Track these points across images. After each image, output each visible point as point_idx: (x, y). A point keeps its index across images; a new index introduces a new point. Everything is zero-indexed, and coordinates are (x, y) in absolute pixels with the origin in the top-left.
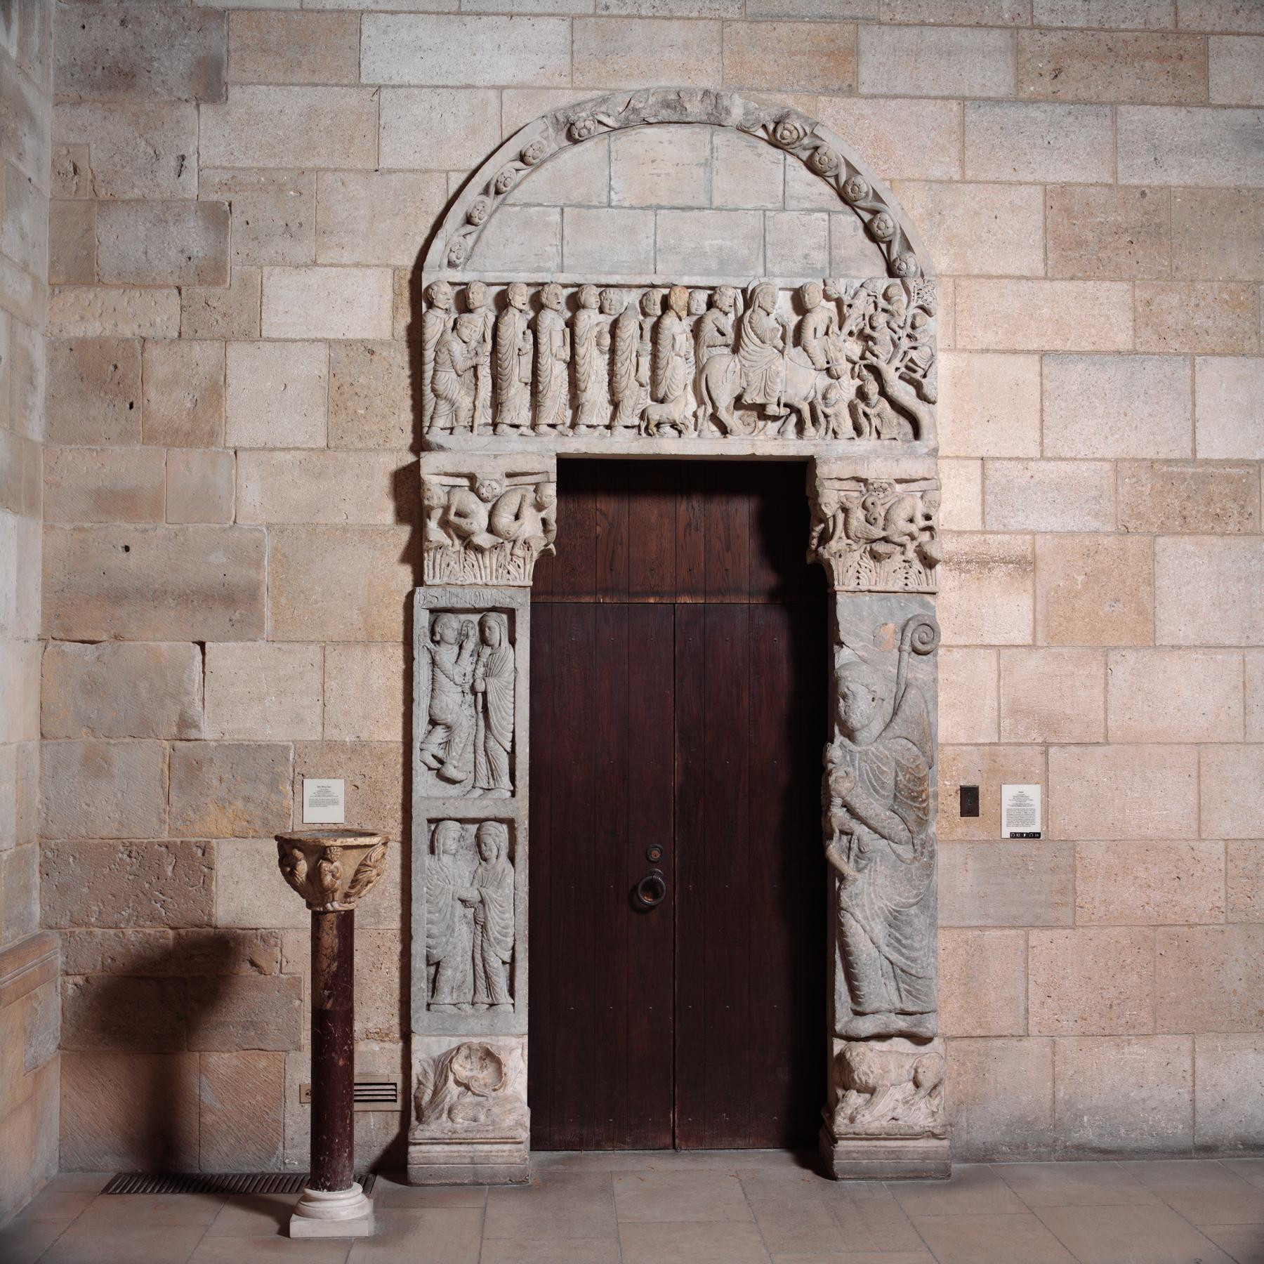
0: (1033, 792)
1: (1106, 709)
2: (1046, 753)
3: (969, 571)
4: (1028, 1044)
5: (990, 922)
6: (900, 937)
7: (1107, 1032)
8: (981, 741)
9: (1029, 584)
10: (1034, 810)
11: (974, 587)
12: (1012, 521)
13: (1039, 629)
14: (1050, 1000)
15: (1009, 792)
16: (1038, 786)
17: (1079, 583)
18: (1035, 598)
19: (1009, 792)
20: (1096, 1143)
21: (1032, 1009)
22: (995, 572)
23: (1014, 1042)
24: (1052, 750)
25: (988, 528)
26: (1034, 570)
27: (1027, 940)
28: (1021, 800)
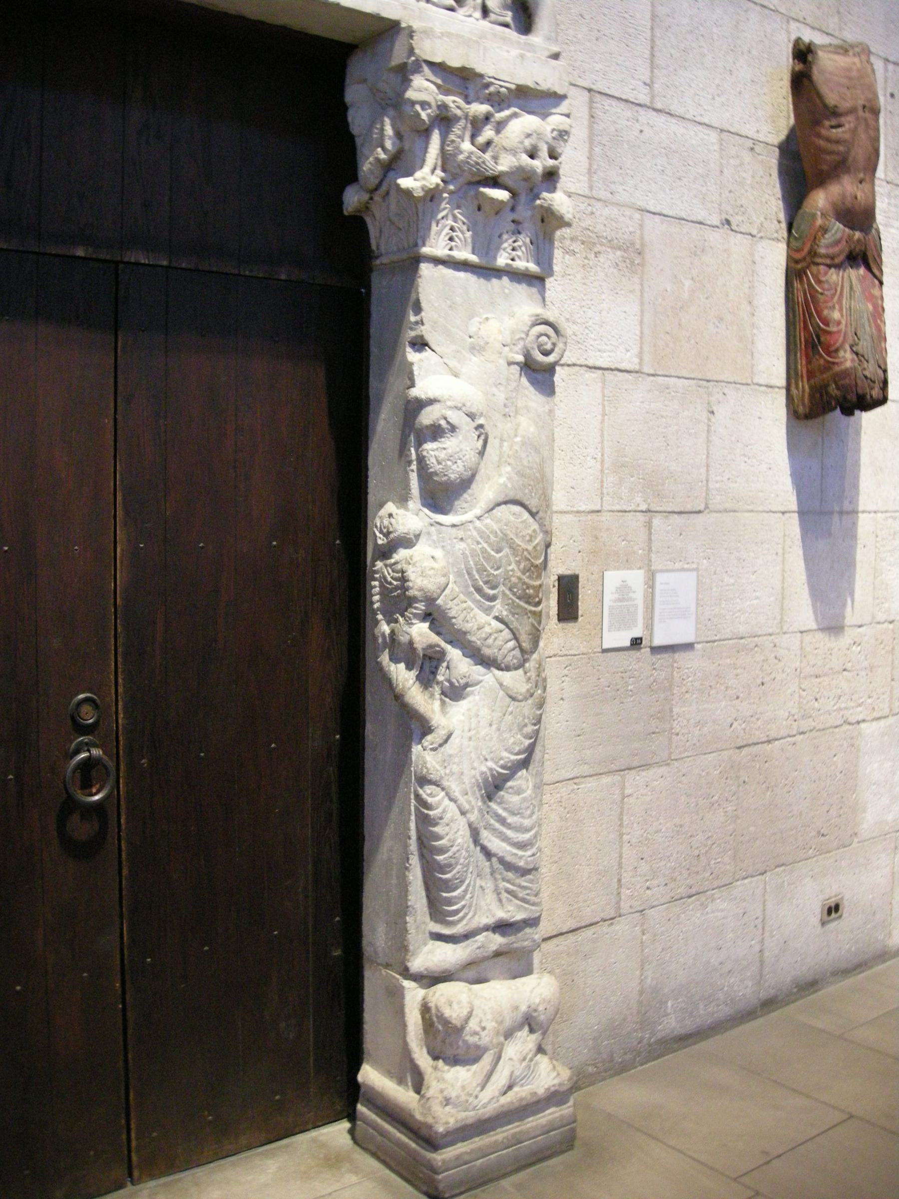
0: (635, 578)
1: (708, 466)
2: (649, 525)
3: (574, 253)
4: (622, 928)
5: (585, 769)
6: (504, 814)
7: (693, 891)
8: (583, 508)
9: (636, 279)
10: (636, 606)
11: (579, 276)
12: (620, 189)
13: (646, 348)
14: (643, 863)
15: (613, 579)
16: (641, 572)
17: (686, 288)
18: (642, 304)
19: (613, 579)
20: (679, 1030)
21: (626, 877)
22: (602, 258)
23: (604, 928)
24: (657, 521)
25: (595, 193)
26: (642, 265)
27: (623, 788)
28: (624, 590)
